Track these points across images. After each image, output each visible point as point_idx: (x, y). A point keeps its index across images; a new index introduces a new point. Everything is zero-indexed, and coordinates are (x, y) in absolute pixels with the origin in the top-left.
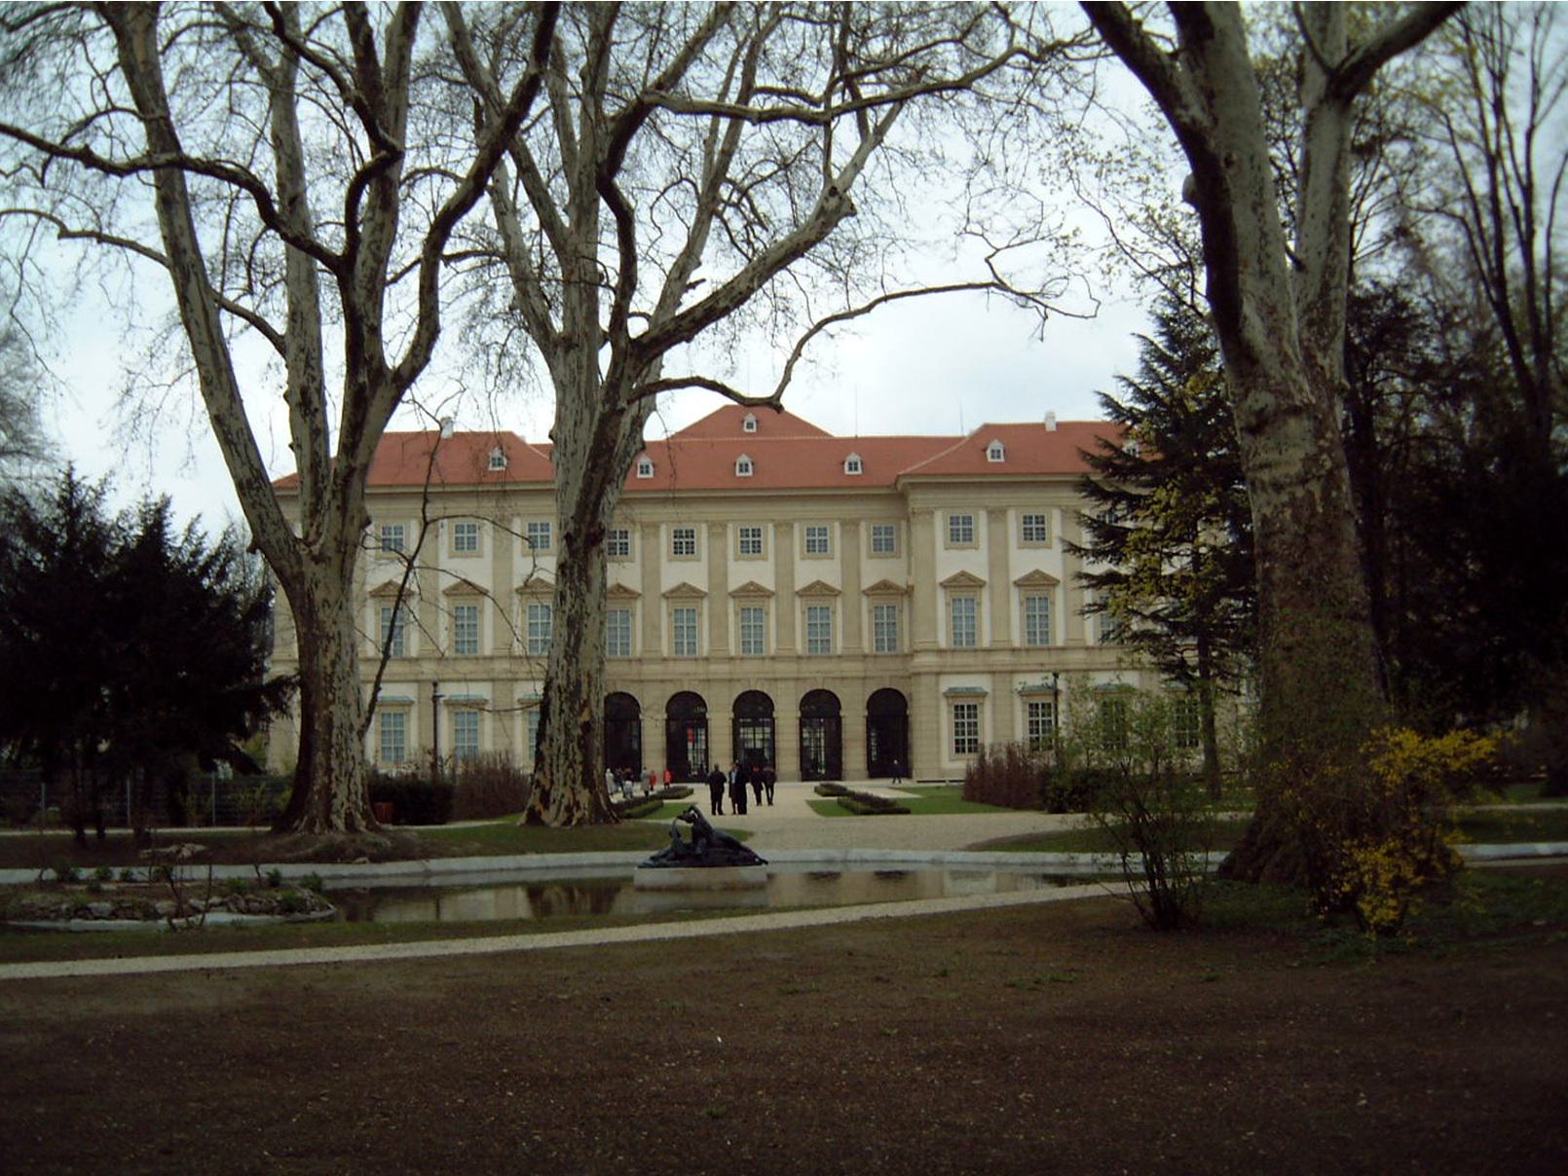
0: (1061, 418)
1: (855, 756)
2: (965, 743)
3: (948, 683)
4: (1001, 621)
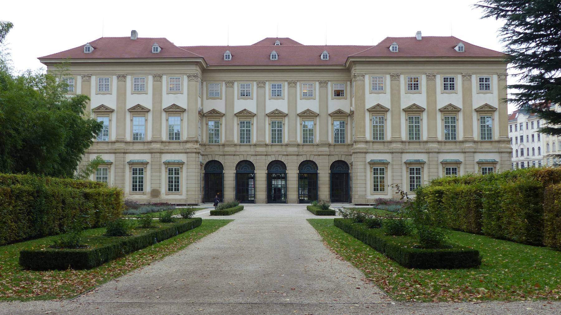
1: (324, 191)
2: (378, 186)
3: (370, 157)
4: (397, 128)
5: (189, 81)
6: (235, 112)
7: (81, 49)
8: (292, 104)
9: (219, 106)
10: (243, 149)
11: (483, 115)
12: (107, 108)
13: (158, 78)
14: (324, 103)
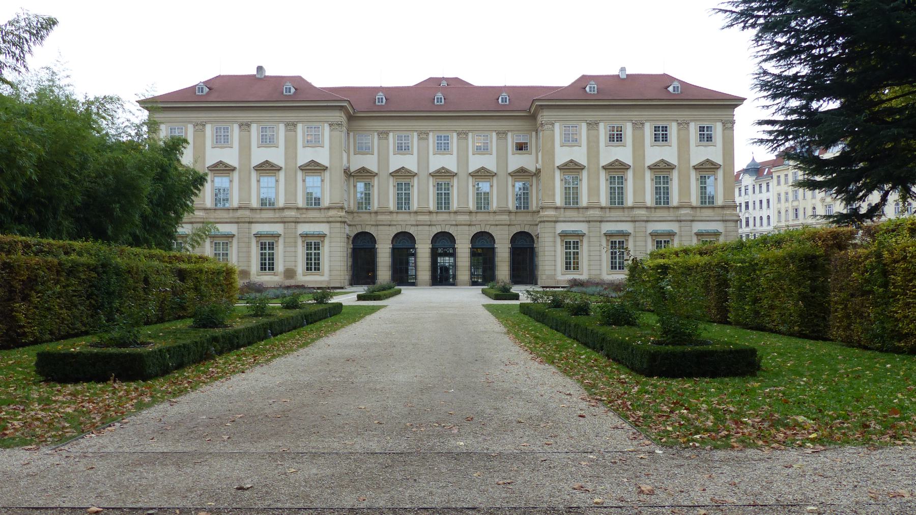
0: (628, 72)
1: (503, 271)
2: (571, 263)
3: (561, 227)
4: (595, 190)
5: (331, 131)
6: (391, 171)
7: (193, 88)
8: (463, 160)
9: (370, 162)
10: (401, 217)
11: (703, 174)
12: (226, 165)
13: (291, 126)
14: (502, 159)
